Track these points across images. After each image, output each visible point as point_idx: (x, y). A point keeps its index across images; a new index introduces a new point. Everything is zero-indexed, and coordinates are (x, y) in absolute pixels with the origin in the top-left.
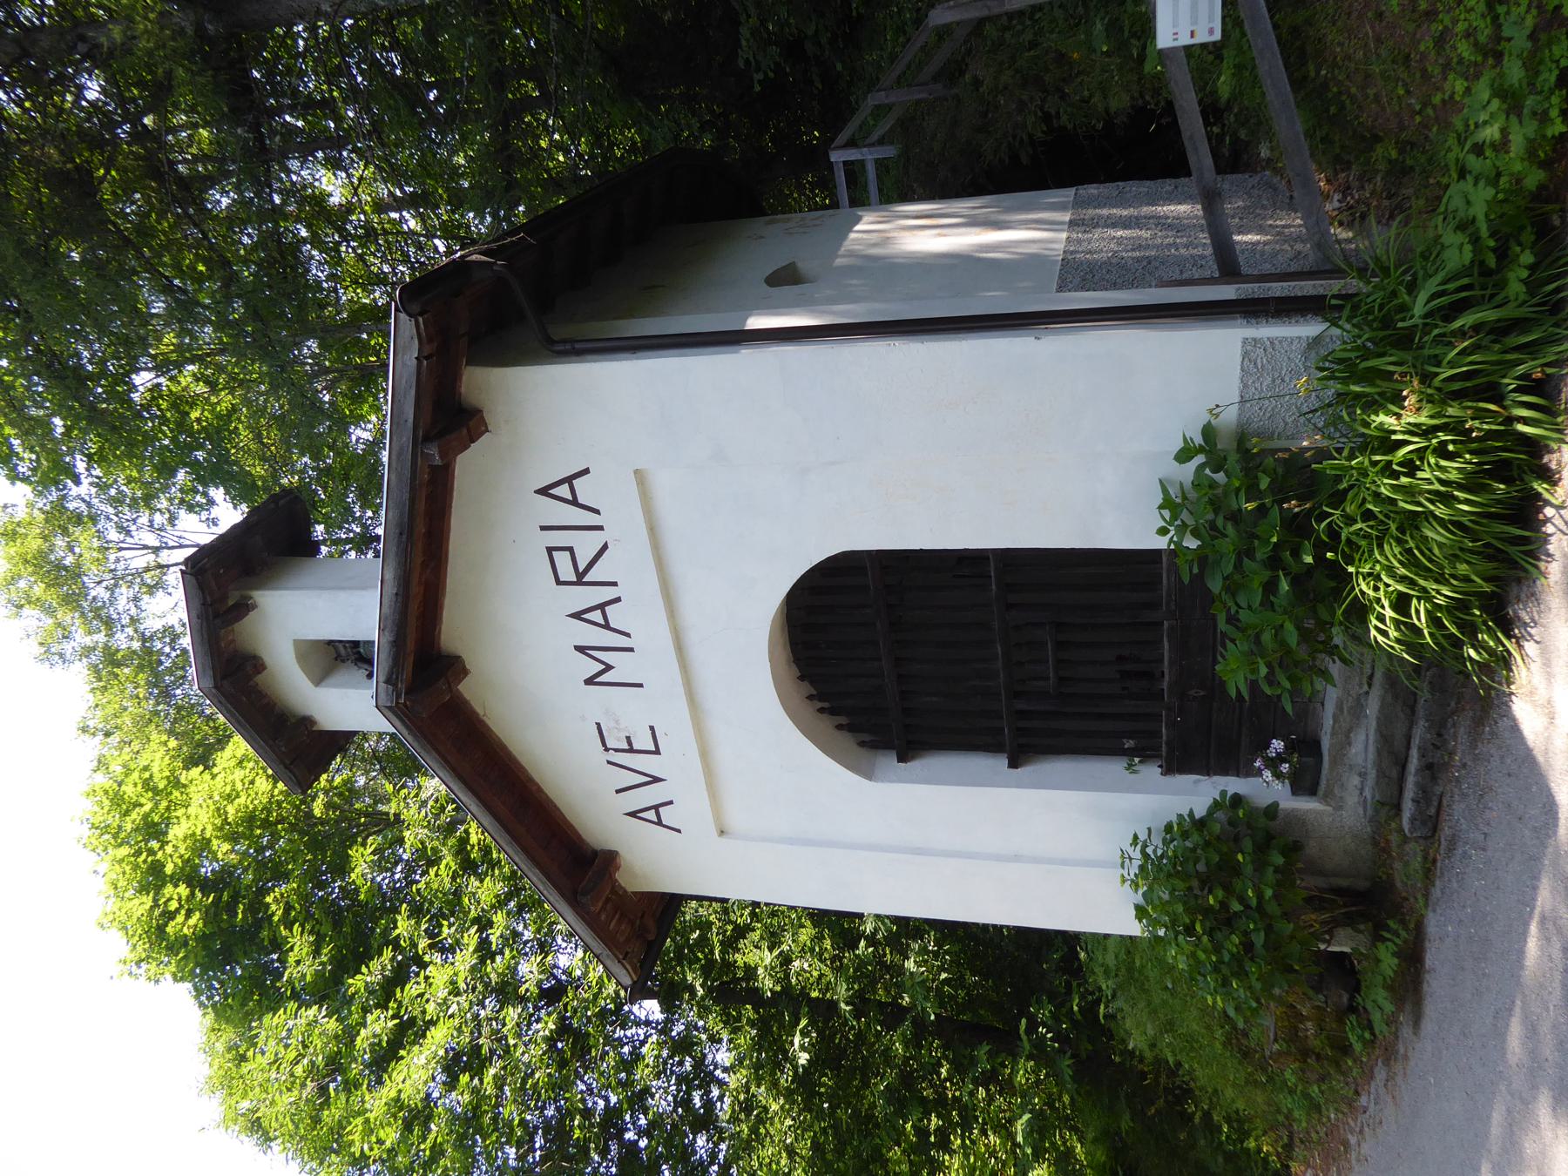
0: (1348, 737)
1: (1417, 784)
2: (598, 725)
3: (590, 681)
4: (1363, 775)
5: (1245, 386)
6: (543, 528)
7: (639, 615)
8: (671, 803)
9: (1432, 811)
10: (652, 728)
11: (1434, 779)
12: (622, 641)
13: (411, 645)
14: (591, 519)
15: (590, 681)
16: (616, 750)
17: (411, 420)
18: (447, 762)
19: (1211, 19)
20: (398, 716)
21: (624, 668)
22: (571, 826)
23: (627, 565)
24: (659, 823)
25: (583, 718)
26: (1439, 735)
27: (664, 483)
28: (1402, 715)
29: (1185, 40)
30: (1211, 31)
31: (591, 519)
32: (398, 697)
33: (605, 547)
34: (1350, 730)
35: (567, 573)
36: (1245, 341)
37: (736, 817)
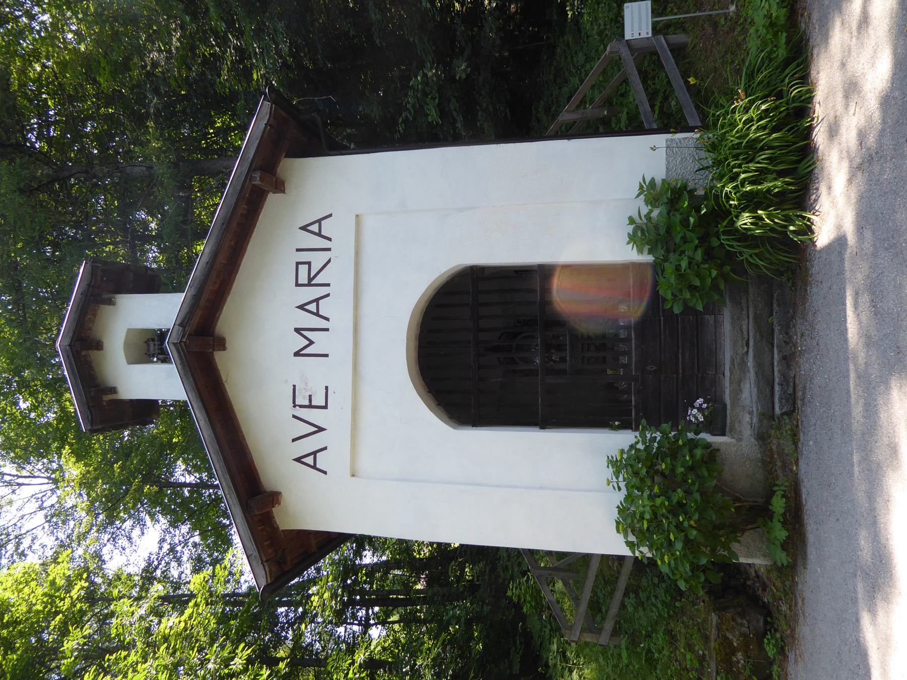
0: (739, 386)
1: (779, 371)
2: (294, 386)
3: (297, 354)
4: (751, 413)
5: (669, 162)
6: (298, 250)
7: (337, 308)
8: (325, 448)
9: (791, 390)
10: (327, 388)
11: (789, 366)
12: (322, 324)
13: (203, 302)
14: (324, 244)
15: (297, 354)
16: (301, 406)
17: (251, 157)
18: (198, 389)
19: (647, 29)
20: (178, 350)
21: (321, 342)
22: (256, 469)
23: (338, 276)
24: (314, 467)
25: (286, 381)
26: (787, 334)
27: (369, 224)
28: (766, 349)
29: (636, 36)
30: (648, 33)
31: (324, 244)
32: (183, 337)
33: (329, 261)
34: (740, 382)
35: (303, 279)
36: (667, 141)
37: (366, 463)
